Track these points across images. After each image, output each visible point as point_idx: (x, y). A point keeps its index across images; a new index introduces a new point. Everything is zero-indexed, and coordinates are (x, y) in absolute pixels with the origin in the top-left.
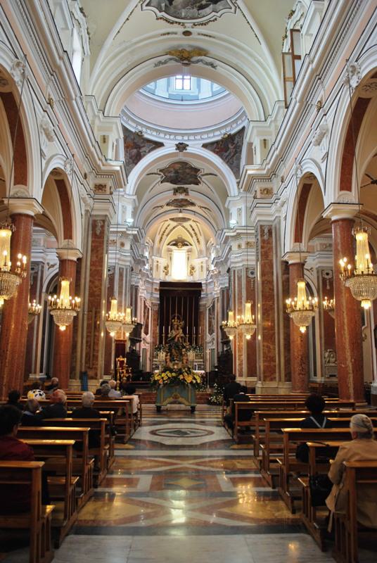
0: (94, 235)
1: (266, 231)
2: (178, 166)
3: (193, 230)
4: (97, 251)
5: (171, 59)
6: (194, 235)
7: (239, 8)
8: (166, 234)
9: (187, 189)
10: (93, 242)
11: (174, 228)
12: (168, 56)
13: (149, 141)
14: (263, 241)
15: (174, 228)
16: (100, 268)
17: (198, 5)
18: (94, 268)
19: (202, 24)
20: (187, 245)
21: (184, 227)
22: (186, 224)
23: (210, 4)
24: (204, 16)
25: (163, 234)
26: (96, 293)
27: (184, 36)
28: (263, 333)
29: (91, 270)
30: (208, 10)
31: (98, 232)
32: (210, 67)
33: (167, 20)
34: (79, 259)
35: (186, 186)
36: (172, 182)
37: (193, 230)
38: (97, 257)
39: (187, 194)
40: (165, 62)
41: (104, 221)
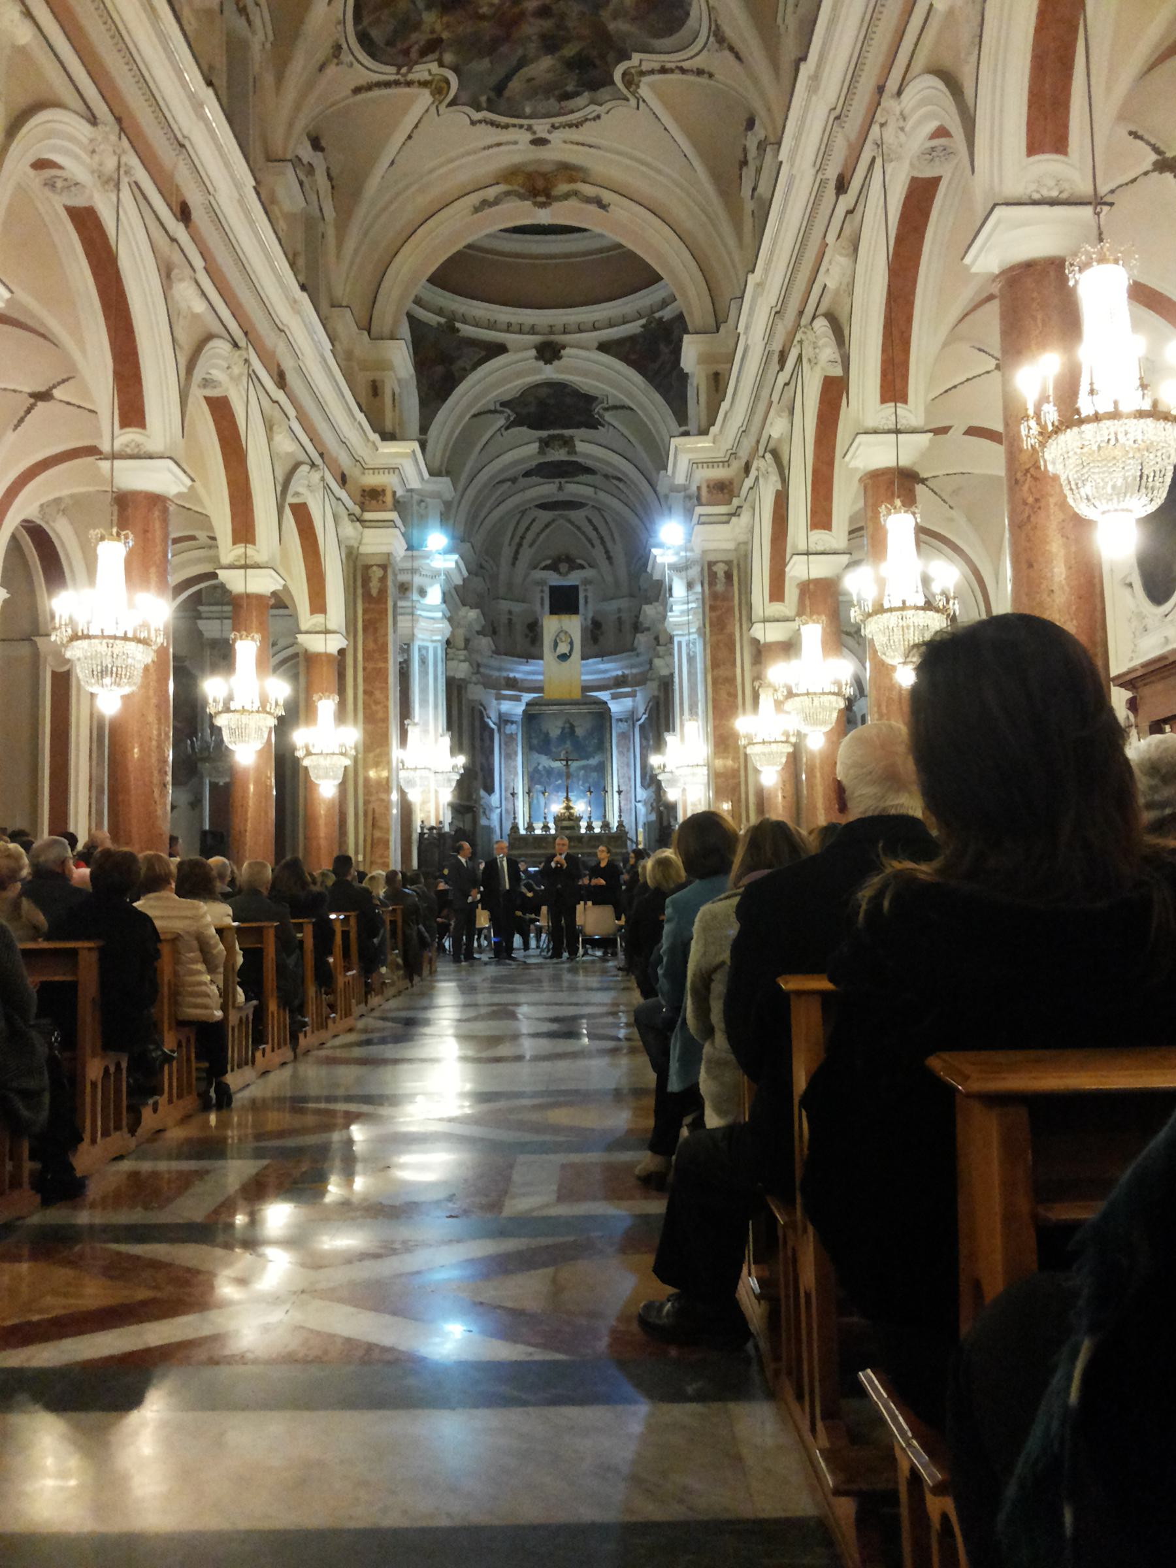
0: (367, 596)
1: (721, 574)
2: (544, 392)
3: (595, 529)
4: (376, 630)
5: (507, 194)
6: (597, 542)
7: (644, 101)
8: (526, 543)
9: (571, 438)
10: (365, 611)
11: (547, 526)
12: (502, 188)
13: (473, 343)
14: (715, 596)
15: (547, 526)
16: (381, 665)
17: (557, 93)
18: (370, 666)
19: (570, 126)
20: (582, 567)
21: (570, 521)
22: (577, 515)
23: (584, 92)
24: (572, 112)
25: (520, 545)
26: (380, 715)
27: (533, 147)
28: (716, 783)
29: (364, 669)
30: (580, 101)
31: (374, 592)
32: (593, 208)
33: (493, 124)
34: (342, 652)
35: (567, 432)
36: (531, 427)
37: (595, 529)
38: (375, 641)
39: (572, 451)
40: (497, 201)
41: (384, 567)
